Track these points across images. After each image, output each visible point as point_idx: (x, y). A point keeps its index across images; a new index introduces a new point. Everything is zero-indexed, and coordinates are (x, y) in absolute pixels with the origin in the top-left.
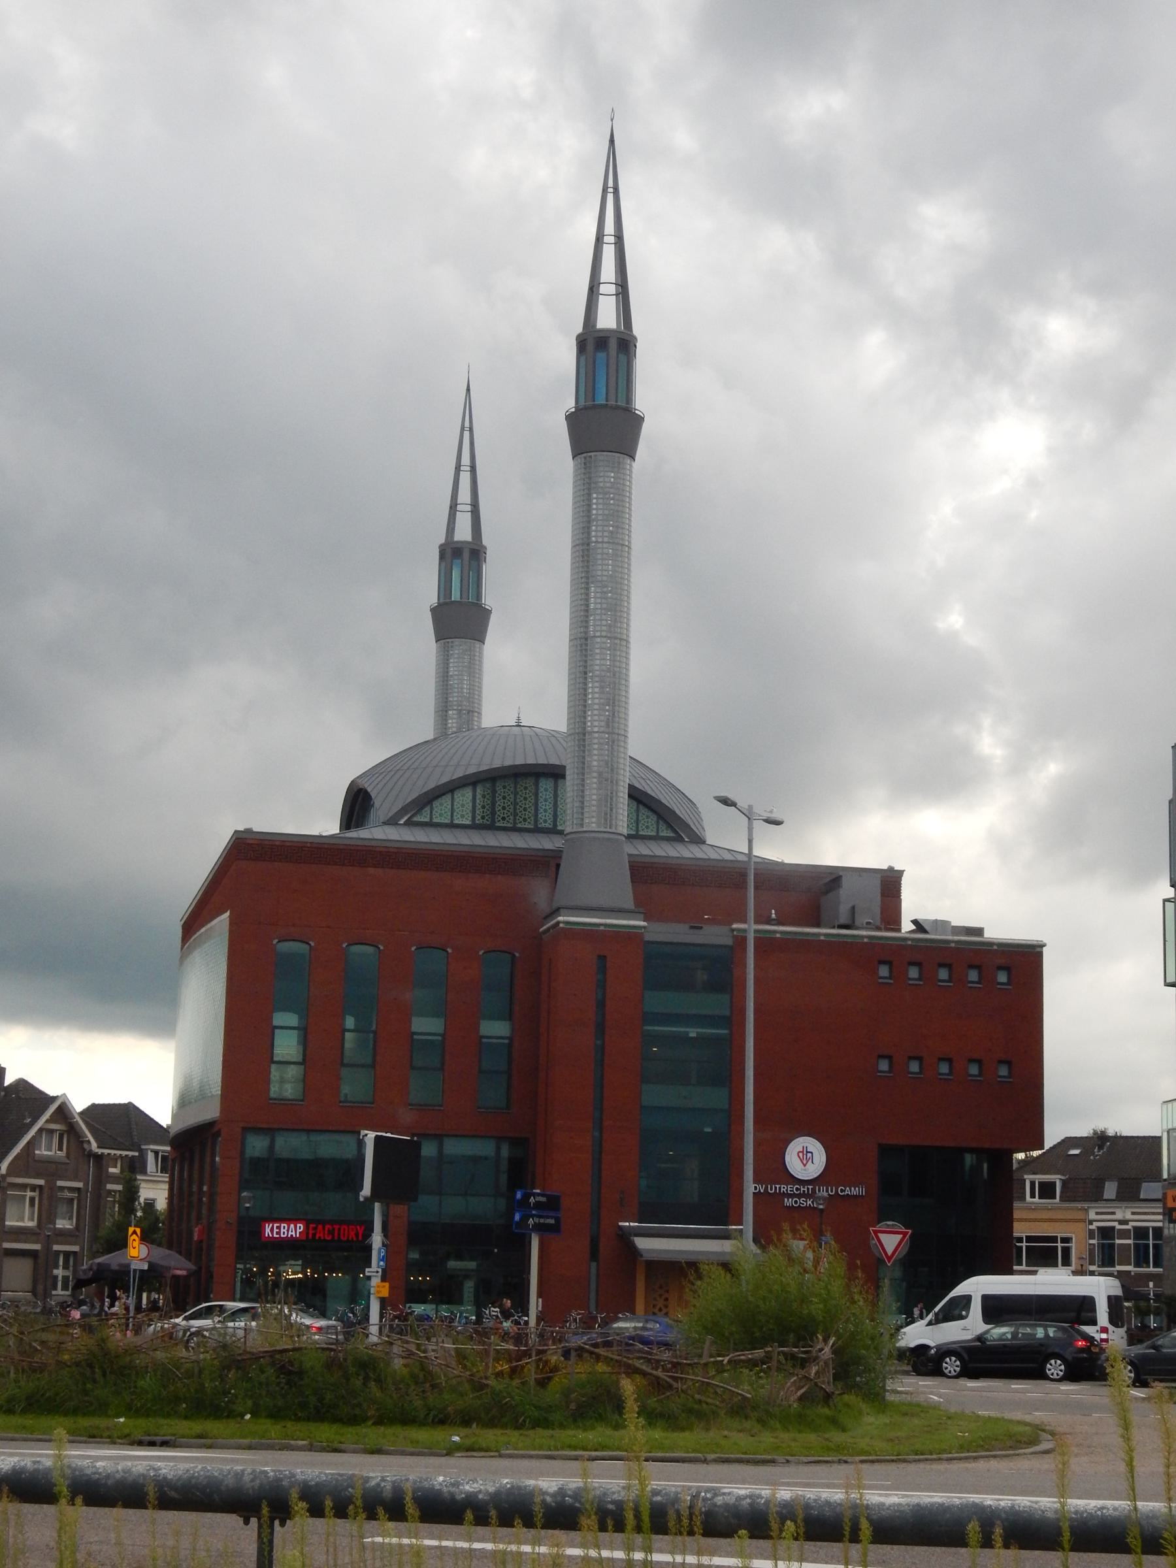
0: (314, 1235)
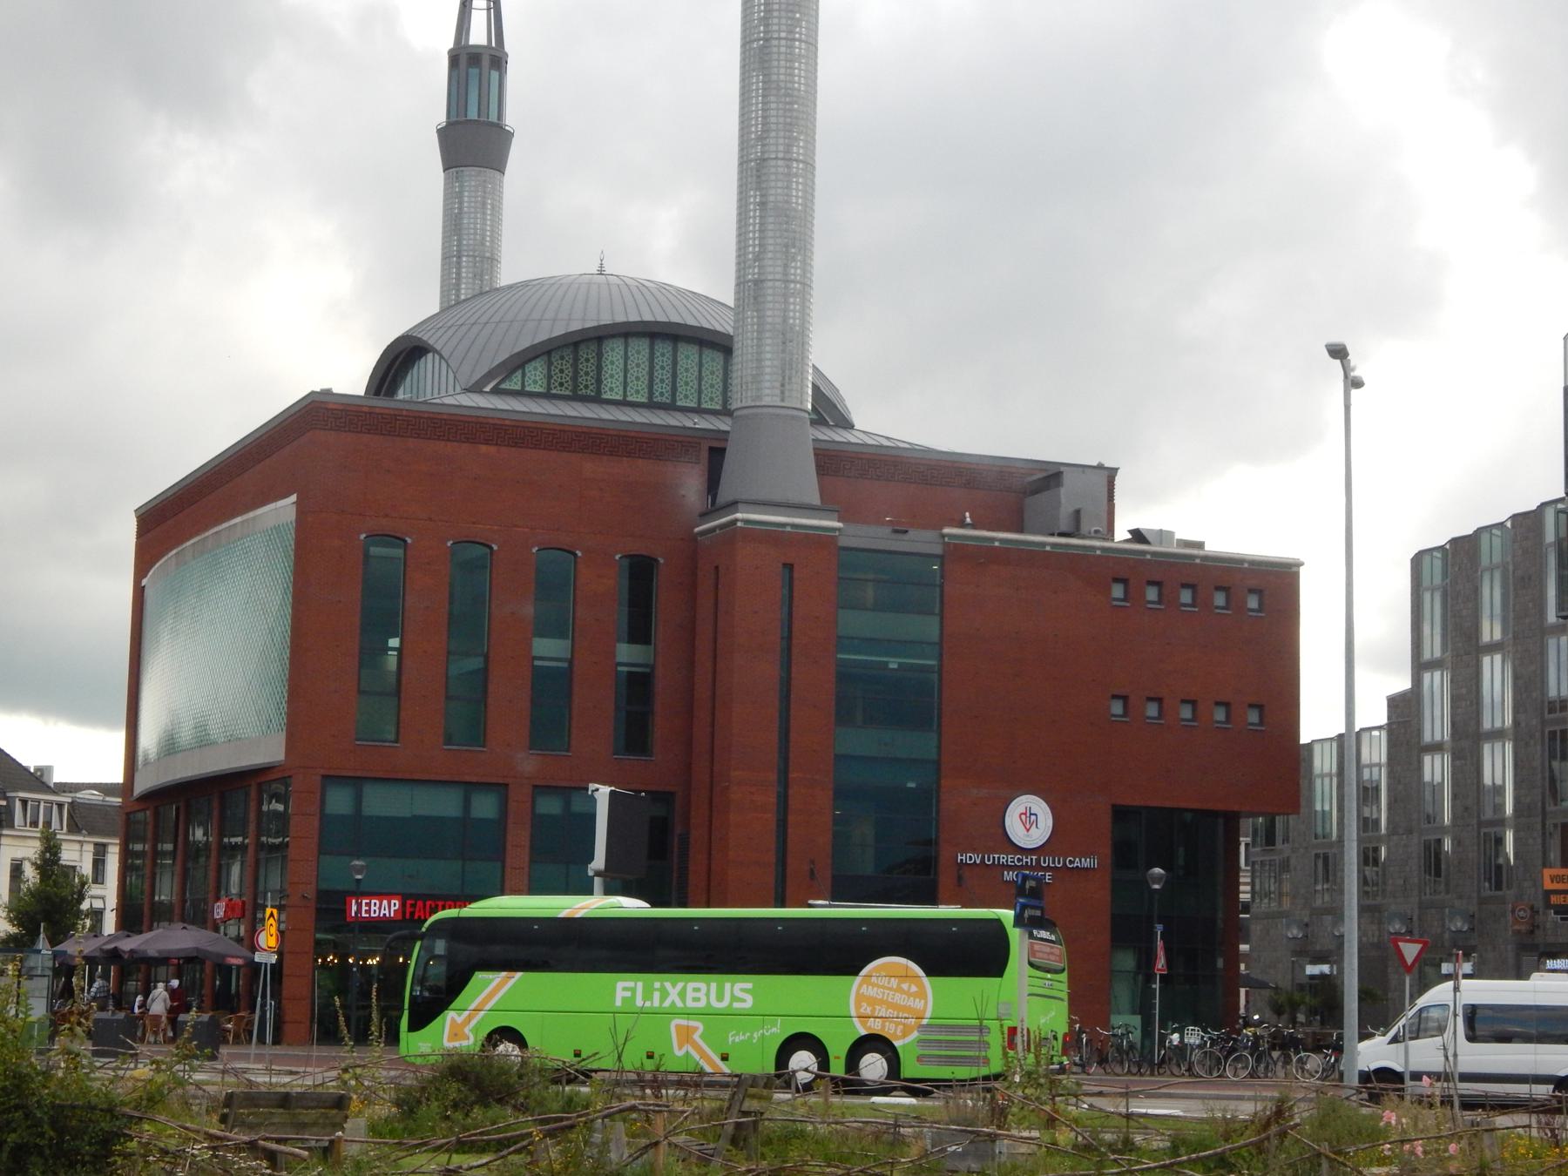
0: (412, 914)
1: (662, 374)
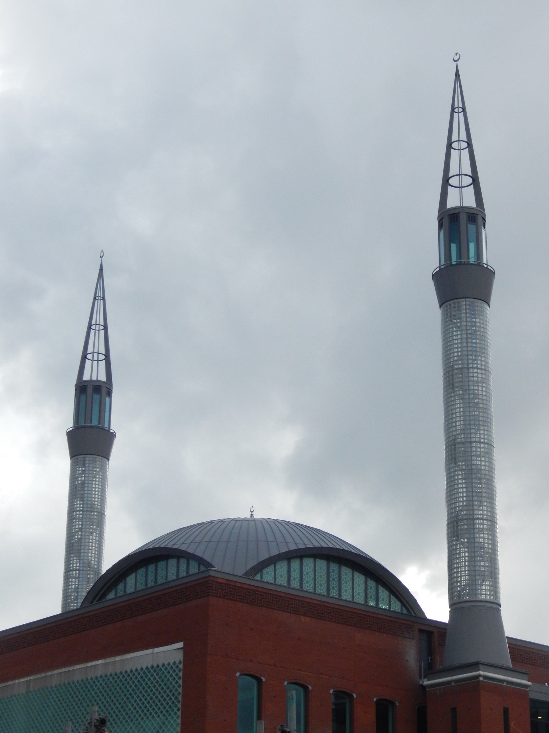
1: (334, 584)
